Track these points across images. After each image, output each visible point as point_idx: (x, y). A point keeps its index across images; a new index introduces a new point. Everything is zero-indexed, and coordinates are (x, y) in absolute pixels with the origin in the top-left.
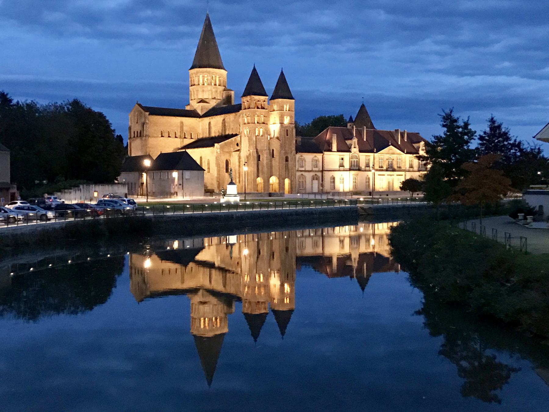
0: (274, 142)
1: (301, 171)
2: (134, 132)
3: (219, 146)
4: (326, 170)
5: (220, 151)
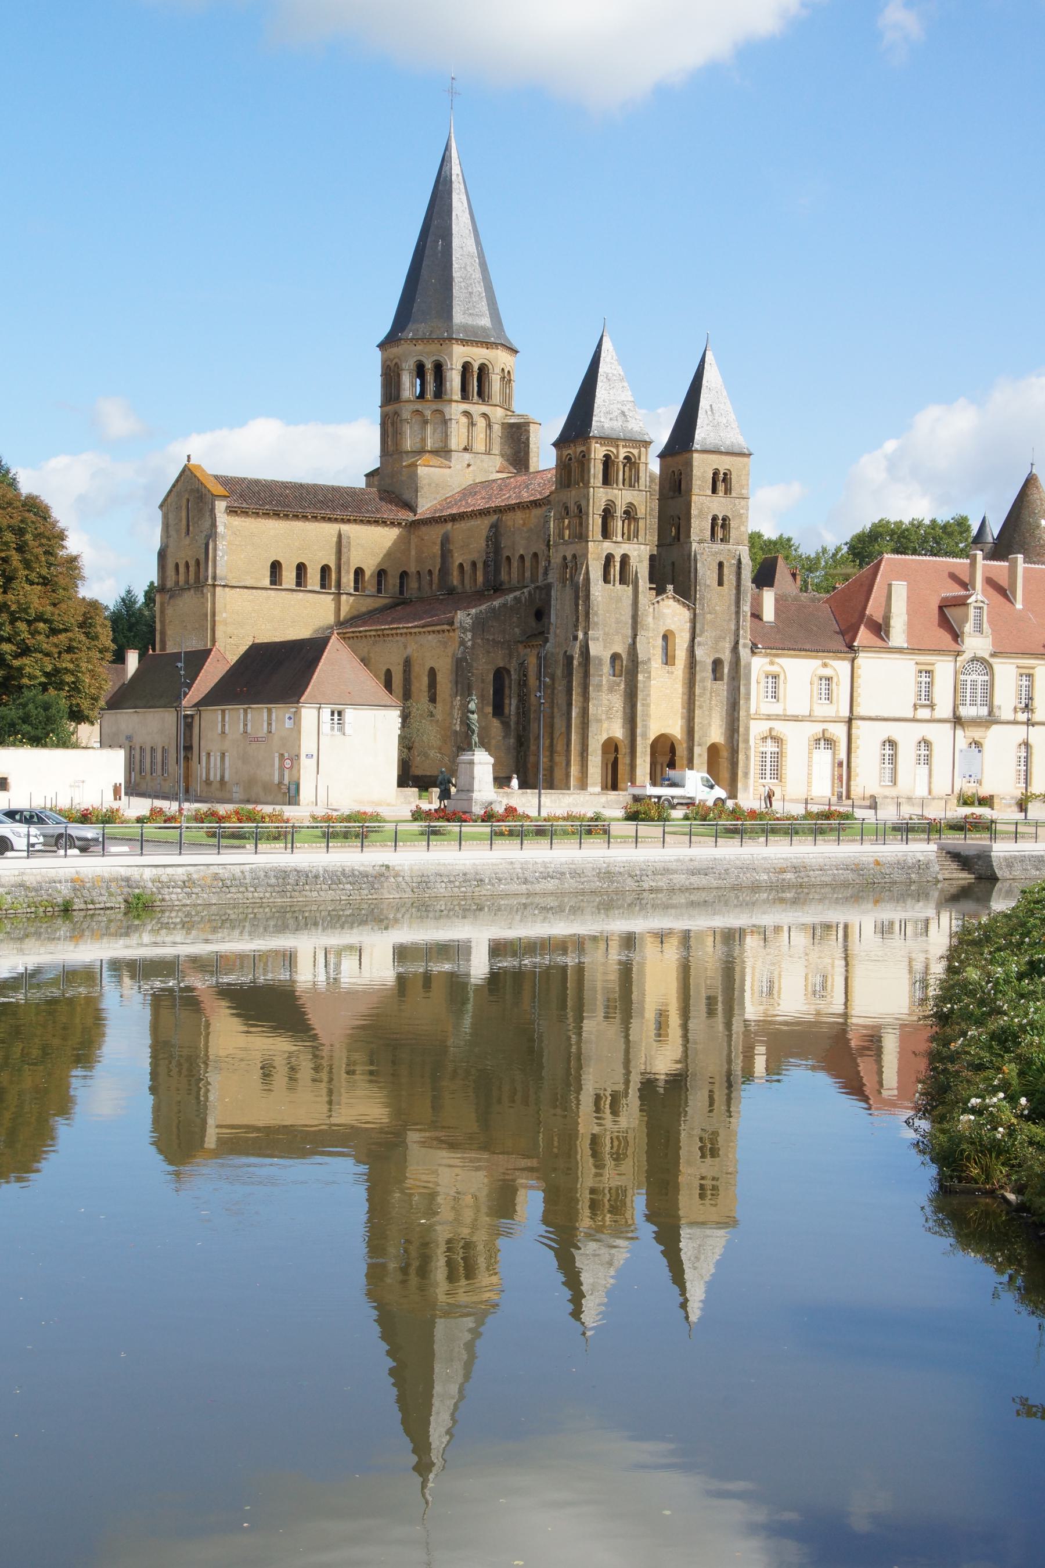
0: (669, 607)
1: (769, 717)
2: (177, 566)
4: (861, 714)
5: (473, 639)
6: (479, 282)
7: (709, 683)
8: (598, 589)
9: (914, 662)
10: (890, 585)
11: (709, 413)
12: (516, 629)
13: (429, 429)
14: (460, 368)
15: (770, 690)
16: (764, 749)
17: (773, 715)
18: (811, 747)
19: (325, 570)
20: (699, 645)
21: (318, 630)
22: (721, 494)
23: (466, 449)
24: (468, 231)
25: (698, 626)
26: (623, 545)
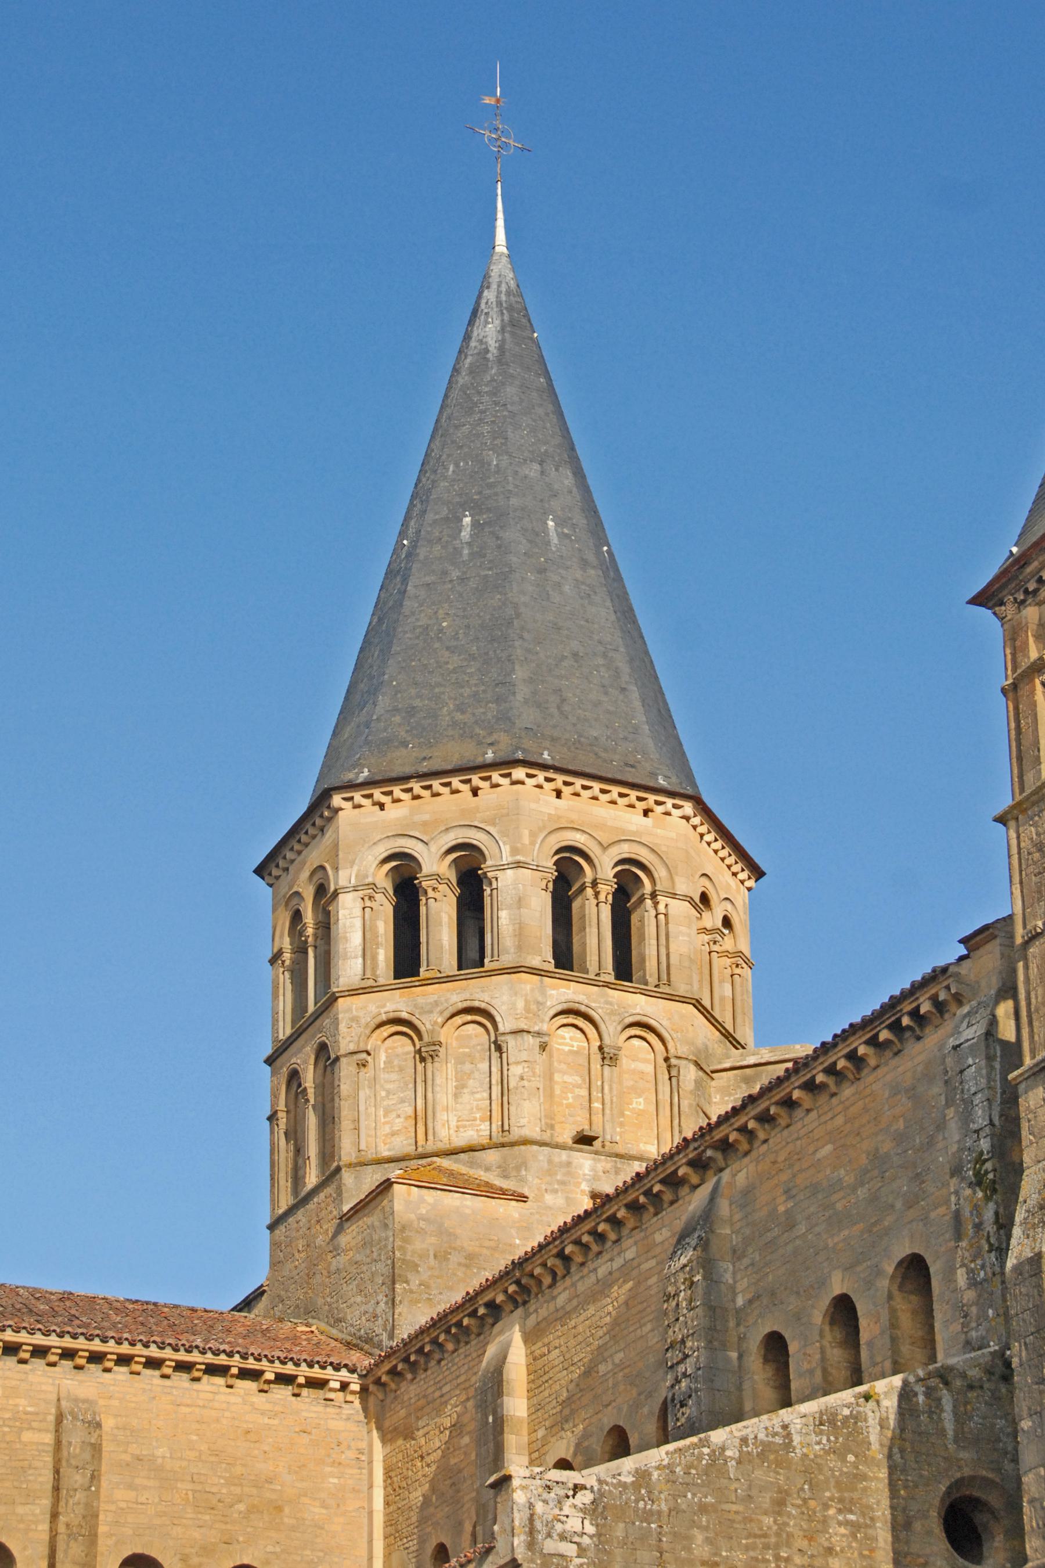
23: (585, 1140)
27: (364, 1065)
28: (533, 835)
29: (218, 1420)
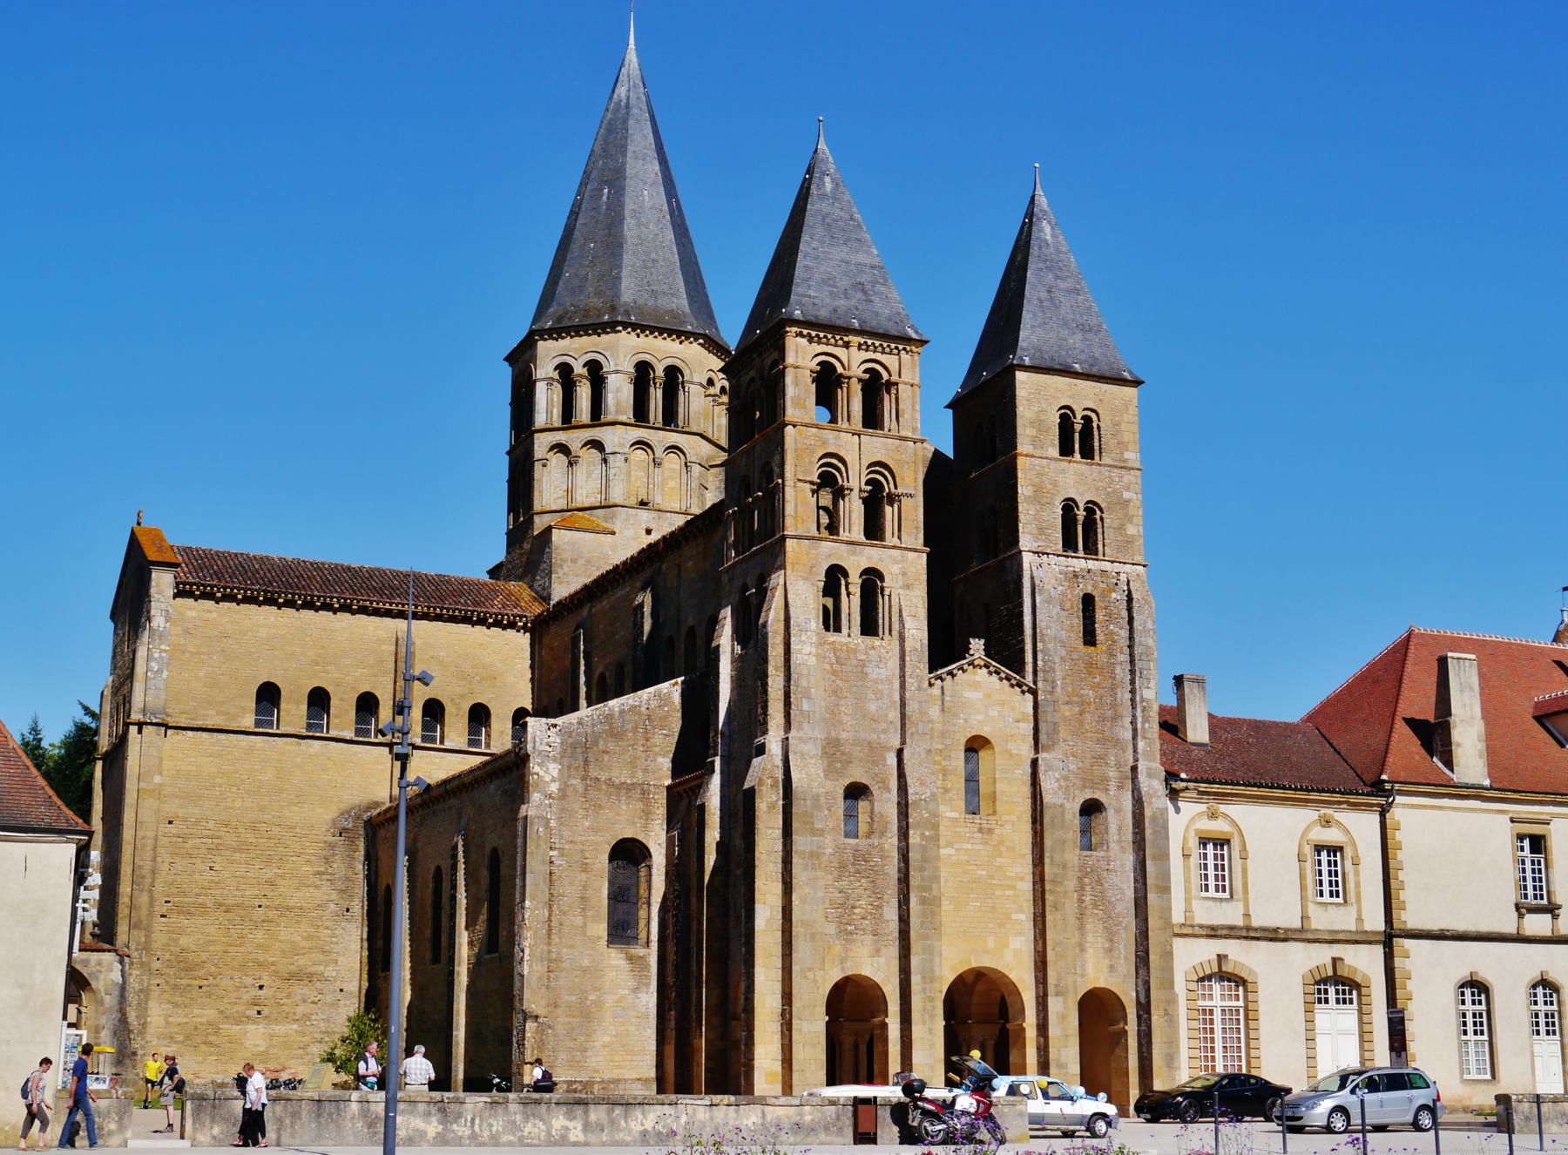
0: (976, 686)
1: (1213, 933)
3: (556, 739)
6: (671, 249)
7: (1073, 855)
8: (809, 644)
9: (1507, 818)
10: (1443, 663)
11: (1046, 304)
12: (660, 760)
13: (580, 470)
14: (633, 371)
15: (1211, 872)
16: (1207, 1003)
17: (1223, 927)
18: (1310, 998)
19: (367, 704)
20: (1049, 768)
21: (348, 812)
22: (1077, 456)
23: (643, 504)
24: (652, 175)
25: (1043, 727)
26: (868, 550)
27: (544, 466)
28: (625, 356)
29: (468, 639)
